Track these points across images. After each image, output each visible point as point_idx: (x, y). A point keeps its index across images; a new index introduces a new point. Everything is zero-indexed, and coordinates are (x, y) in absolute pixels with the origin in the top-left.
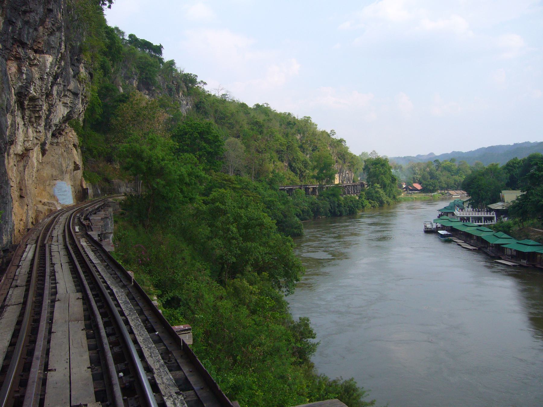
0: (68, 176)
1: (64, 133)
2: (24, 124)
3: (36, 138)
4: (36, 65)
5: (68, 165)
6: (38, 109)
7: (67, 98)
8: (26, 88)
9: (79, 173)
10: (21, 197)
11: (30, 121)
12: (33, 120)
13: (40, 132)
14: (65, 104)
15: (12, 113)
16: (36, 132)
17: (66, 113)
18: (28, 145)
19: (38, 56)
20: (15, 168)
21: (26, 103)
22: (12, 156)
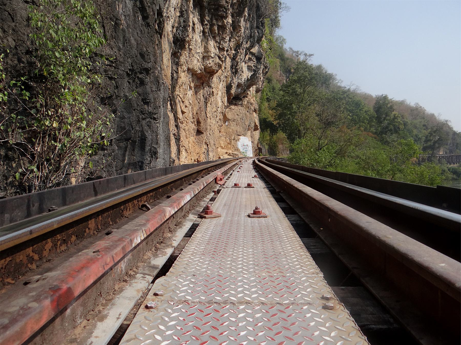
3: (219, 58)
10: (199, 132)
11: (211, 30)
12: (216, 28)
16: (219, 48)
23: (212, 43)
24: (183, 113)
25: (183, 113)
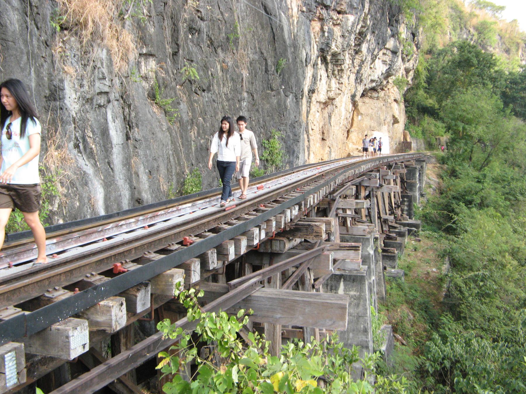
0: (385, 128)
1: (386, 89)
2: (328, 76)
3: (339, 89)
4: (339, 24)
5: (386, 117)
6: (339, 63)
7: (386, 56)
8: (328, 45)
9: (400, 127)
11: (333, 74)
12: (336, 72)
13: (342, 83)
14: (384, 62)
15: (315, 65)
16: (339, 83)
17: (385, 70)
18: (332, 95)
19: (340, 16)
20: (318, 114)
21: (329, 58)
22: (314, 103)
23: (333, 81)
24: (312, 129)
25: (312, 129)
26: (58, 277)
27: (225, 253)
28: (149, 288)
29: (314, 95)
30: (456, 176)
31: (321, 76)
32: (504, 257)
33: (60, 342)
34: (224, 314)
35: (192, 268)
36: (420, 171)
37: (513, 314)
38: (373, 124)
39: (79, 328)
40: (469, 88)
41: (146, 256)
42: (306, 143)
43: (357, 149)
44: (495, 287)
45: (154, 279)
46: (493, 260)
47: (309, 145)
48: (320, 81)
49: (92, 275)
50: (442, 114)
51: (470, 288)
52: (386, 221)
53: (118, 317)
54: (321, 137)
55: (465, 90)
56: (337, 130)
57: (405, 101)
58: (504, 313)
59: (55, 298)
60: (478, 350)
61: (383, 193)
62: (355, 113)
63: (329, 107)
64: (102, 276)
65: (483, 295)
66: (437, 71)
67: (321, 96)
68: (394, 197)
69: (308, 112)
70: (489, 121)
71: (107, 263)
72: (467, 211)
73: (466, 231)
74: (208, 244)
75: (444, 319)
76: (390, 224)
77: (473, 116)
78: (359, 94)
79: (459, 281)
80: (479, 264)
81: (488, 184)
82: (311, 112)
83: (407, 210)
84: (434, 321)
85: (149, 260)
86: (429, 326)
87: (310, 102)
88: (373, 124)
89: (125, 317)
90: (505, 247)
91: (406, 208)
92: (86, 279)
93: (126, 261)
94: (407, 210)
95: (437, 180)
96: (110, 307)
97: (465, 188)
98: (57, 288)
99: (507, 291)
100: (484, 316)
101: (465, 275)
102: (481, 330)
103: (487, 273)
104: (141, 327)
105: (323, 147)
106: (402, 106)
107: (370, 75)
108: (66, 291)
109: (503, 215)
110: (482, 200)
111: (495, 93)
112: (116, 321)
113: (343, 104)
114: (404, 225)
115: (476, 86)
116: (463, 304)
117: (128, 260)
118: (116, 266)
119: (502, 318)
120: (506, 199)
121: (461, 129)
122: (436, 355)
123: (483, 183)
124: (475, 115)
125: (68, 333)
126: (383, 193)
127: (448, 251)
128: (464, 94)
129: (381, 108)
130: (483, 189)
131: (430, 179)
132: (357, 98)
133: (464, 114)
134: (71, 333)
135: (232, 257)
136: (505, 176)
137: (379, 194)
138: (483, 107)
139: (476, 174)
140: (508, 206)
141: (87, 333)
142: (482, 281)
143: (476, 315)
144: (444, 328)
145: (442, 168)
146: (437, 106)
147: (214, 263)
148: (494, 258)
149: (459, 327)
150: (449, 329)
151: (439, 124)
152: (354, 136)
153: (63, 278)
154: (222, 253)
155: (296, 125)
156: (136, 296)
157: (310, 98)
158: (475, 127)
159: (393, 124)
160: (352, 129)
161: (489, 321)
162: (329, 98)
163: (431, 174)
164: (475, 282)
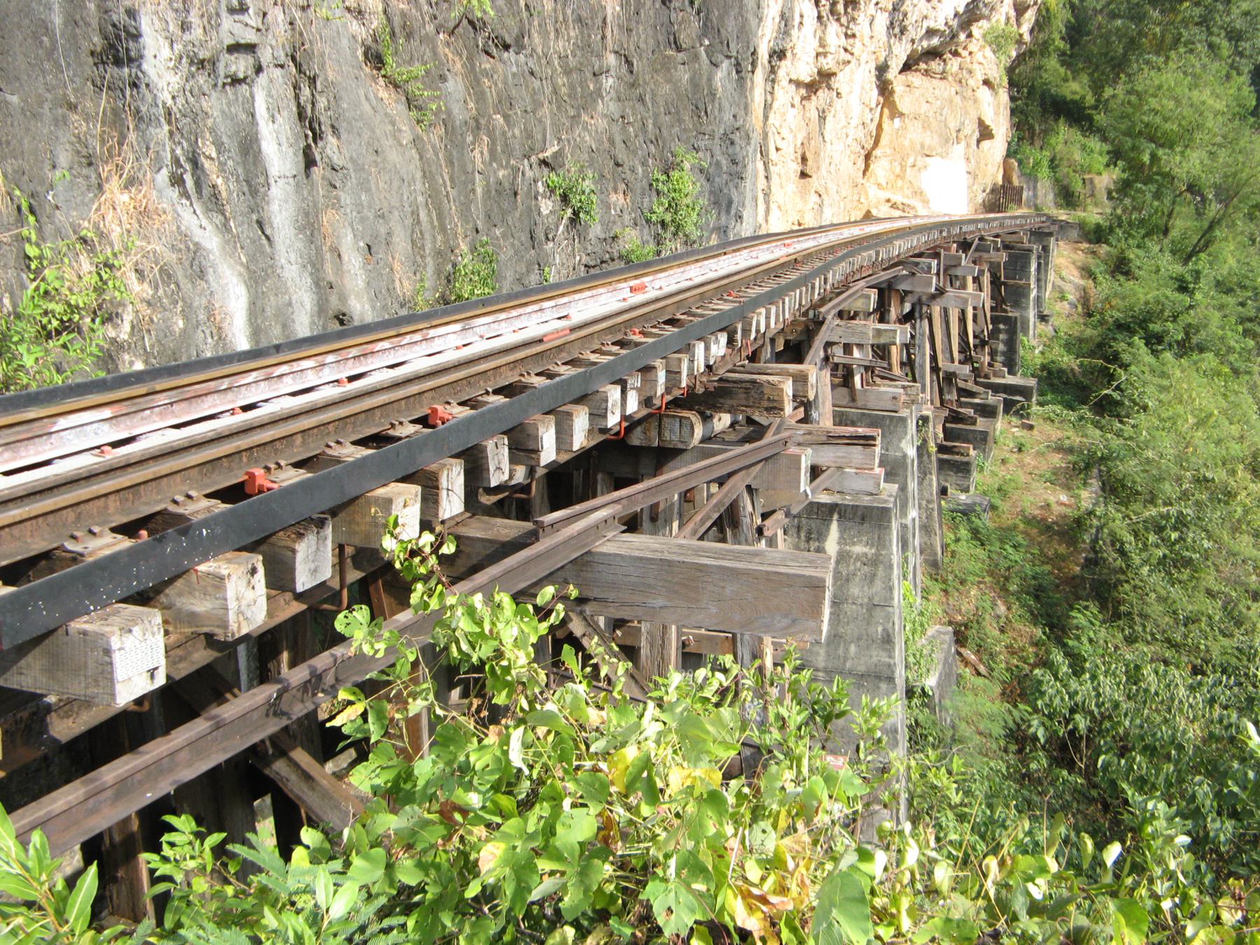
1: (965, 53)
2: (820, 18)
3: (846, 50)
9: (997, 148)
13: (854, 36)
16: (846, 35)
18: (828, 63)
20: (792, 112)
22: (784, 83)
23: (833, 28)
24: (777, 149)
25: (777, 149)
26: (101, 502)
27: (531, 446)
28: (329, 531)
29: (783, 63)
30: (1127, 274)
31: (802, 16)
32: (1233, 472)
33: (91, 664)
34: (505, 599)
35: (444, 483)
36: (1039, 257)
37: (1244, 610)
38: (930, 139)
39: (136, 630)
40: (1173, 54)
41: (329, 452)
42: (762, 183)
43: (888, 201)
44: (1206, 544)
45: (341, 506)
46: (1206, 480)
47: (769, 188)
48: (799, 29)
49: (189, 497)
50: (1100, 118)
51: (1145, 545)
52: (950, 377)
53: (244, 603)
54: (799, 168)
55: (1162, 59)
56: (838, 153)
57: (1012, 84)
58: (1225, 608)
59: (91, 554)
60: (1157, 694)
61: (945, 312)
62: (886, 111)
63: (820, 93)
64: (214, 501)
65: (1176, 563)
66: (1094, 10)
67: (802, 66)
68: (975, 320)
69: (767, 107)
70: (1219, 139)
71: (230, 469)
72: (1149, 359)
73: (1145, 408)
74: (487, 424)
75: (1079, 615)
76: (961, 384)
77: (1180, 125)
78: (896, 64)
79: (1120, 526)
80: (1168, 488)
81: (1206, 295)
82: (775, 105)
83: (1003, 354)
84: (1055, 621)
85: (337, 461)
86: (1044, 633)
87: (773, 81)
88: (930, 139)
89: (263, 603)
90: (1236, 449)
91: (1001, 347)
92: (173, 508)
93: (277, 464)
94: (1003, 354)
95: (1082, 282)
96: (222, 578)
97: (1147, 303)
98: (96, 529)
99: (1234, 555)
100: (1174, 613)
101: (1136, 513)
102: (1166, 645)
103: (1189, 511)
104: (308, 629)
105: (803, 193)
106: (1004, 96)
107: (926, 17)
108: (120, 537)
109: (1236, 372)
110: (1187, 334)
111: (1237, 69)
112: (240, 612)
113: (856, 85)
114: (997, 389)
115: (1191, 51)
116: (1127, 582)
117: (283, 463)
118: (252, 476)
119: (1217, 618)
120: (1246, 333)
121: (1146, 158)
122: (1057, 701)
123: (1191, 293)
124: (1184, 123)
125: (108, 643)
126: (945, 312)
127: (1099, 454)
128: (1159, 69)
129: (951, 102)
130: (1191, 307)
131: (1062, 278)
132: (892, 74)
133: (1158, 120)
134: (115, 642)
135: (549, 453)
136: (1247, 277)
137: (936, 310)
138: (1204, 103)
139: (1178, 269)
140: (1250, 351)
141: (159, 641)
142: (1175, 529)
143: (1156, 609)
144: (1078, 638)
145: (1094, 253)
146: (1090, 100)
147: (501, 468)
148: (1209, 475)
149: (1114, 636)
150: (1091, 641)
151: (1095, 143)
152: (880, 167)
153: (112, 502)
154: (522, 447)
155: (736, 137)
156: (294, 551)
157: (773, 70)
158: (1182, 153)
159: (978, 142)
160: (877, 152)
161: (1185, 625)
162: (820, 73)
163: (1067, 267)
164: (1160, 530)
